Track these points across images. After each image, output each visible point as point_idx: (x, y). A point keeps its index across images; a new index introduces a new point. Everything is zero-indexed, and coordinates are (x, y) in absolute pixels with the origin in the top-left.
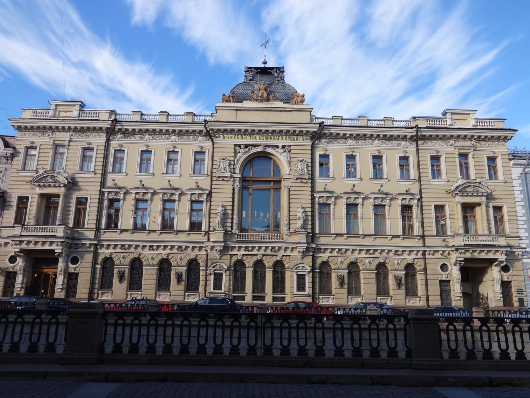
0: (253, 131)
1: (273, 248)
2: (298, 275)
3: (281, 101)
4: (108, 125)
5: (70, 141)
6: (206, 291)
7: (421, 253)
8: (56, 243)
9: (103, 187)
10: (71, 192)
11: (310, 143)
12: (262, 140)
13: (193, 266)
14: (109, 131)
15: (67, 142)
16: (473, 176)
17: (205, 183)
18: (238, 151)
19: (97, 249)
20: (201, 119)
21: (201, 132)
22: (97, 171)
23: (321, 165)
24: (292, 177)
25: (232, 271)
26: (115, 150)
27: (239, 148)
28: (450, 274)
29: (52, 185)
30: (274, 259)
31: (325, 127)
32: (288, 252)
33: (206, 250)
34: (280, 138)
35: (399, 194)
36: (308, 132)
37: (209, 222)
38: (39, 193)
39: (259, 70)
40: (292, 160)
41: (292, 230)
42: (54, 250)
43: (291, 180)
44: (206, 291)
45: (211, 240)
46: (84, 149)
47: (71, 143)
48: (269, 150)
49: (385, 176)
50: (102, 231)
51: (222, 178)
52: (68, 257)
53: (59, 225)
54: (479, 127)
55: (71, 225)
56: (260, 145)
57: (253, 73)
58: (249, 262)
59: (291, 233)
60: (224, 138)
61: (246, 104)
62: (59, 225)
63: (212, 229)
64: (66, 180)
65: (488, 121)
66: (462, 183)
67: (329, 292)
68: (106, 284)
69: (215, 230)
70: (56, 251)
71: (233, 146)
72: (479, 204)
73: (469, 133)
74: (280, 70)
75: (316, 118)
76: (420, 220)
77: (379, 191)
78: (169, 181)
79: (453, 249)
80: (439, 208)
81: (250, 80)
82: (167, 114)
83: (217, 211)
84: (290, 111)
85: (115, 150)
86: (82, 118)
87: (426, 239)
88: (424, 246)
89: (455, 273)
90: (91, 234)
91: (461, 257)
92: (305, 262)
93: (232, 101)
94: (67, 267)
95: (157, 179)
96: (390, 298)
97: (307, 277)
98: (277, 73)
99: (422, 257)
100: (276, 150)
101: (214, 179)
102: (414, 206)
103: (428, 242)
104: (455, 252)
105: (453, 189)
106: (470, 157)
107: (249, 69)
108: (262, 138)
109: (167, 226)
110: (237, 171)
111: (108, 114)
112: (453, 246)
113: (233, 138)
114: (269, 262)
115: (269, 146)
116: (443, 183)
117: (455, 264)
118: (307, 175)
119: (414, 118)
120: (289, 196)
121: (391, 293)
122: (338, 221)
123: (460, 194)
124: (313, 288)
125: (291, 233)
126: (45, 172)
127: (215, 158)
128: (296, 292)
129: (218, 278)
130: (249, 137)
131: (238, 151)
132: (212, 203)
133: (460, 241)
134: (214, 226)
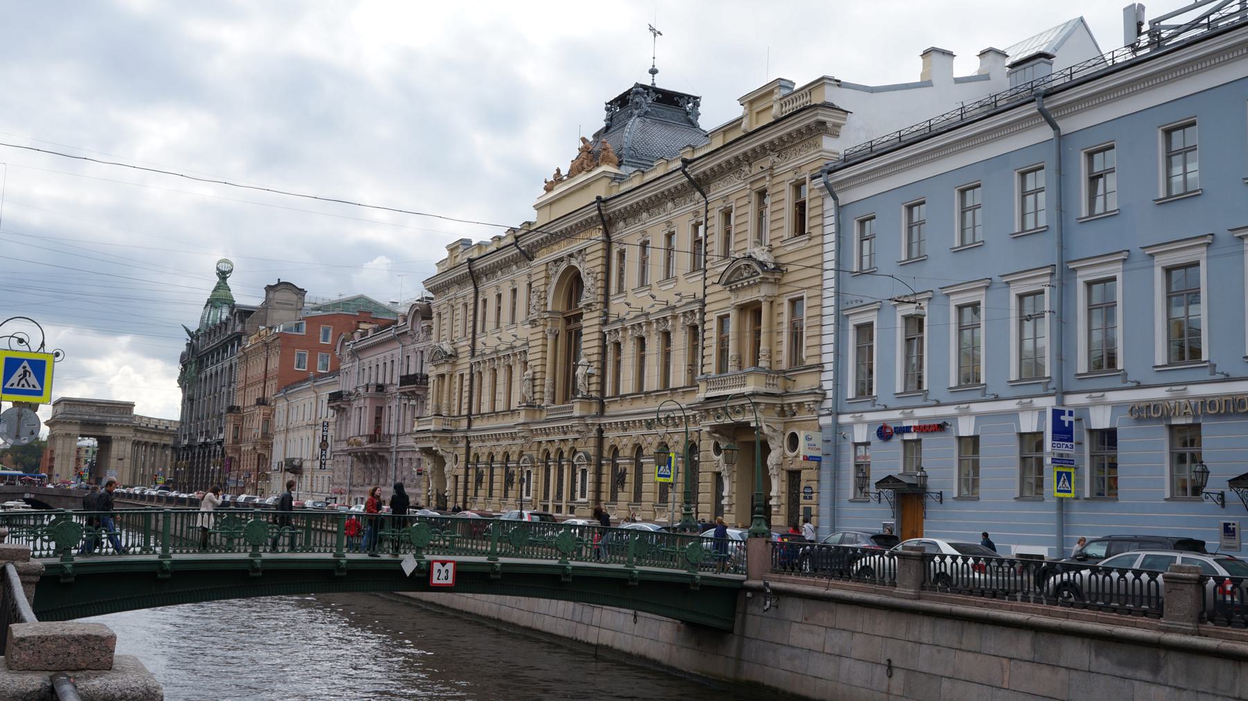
19: (468, 442)
32: (577, 436)
48: (574, 262)
71: (544, 267)
80: (723, 320)
84: (588, 186)
90: (464, 424)
124: (598, 491)
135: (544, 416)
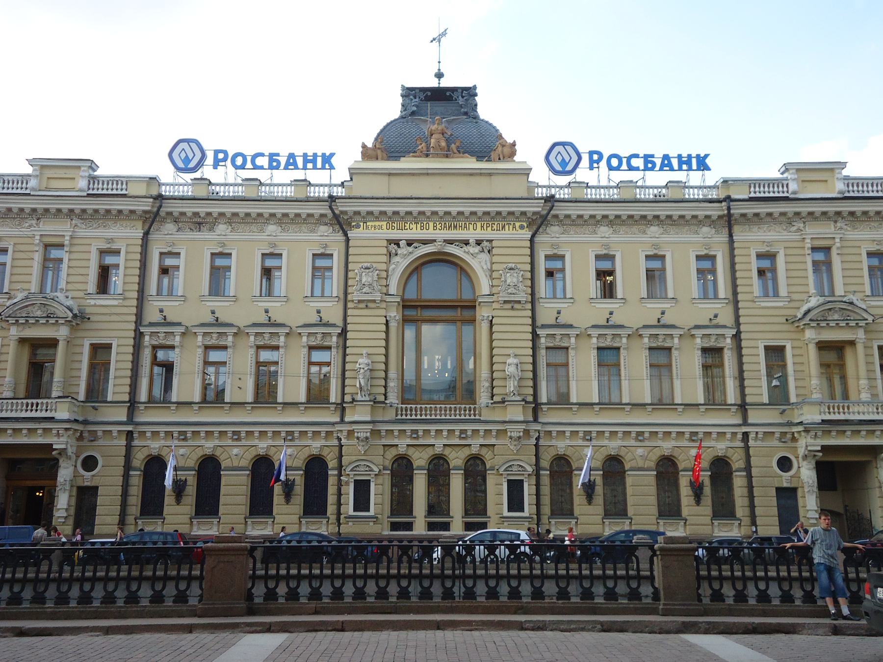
0: (422, 213)
1: (463, 432)
2: (510, 482)
3: (472, 153)
4: (147, 205)
5: (72, 237)
6: (339, 514)
7: (740, 436)
8: (54, 432)
9: (141, 325)
10: (80, 334)
11: (527, 234)
12: (438, 231)
13: (315, 468)
14: (147, 216)
15: (67, 238)
16: (839, 290)
17: (333, 314)
18: (394, 251)
20: (324, 193)
21: (322, 215)
22: (128, 294)
23: (550, 274)
24: (494, 298)
25: (387, 477)
26: (161, 254)
27: (395, 247)
28: (797, 476)
29: (43, 321)
30: (466, 452)
31: (556, 204)
32: (492, 441)
33: (340, 439)
34: (471, 226)
35: (697, 327)
36: (524, 213)
37: (343, 386)
38: (17, 338)
39: (429, 94)
40: (495, 267)
41: (496, 399)
42: (52, 445)
43: (495, 305)
44: (339, 514)
45: (347, 419)
46: (103, 252)
47: (76, 241)
49: (670, 294)
50: (142, 407)
51: (366, 304)
52: (78, 457)
53: (59, 397)
54: (851, 194)
55: (82, 397)
56: (435, 241)
57: (417, 100)
58: (420, 459)
59: (495, 403)
60: (367, 227)
61: (406, 164)
62: (59, 397)
63: (348, 398)
64: (68, 312)
65: (870, 182)
66: (818, 303)
67: (570, 514)
68: (152, 505)
69: (354, 400)
70: (54, 447)
71: (385, 243)
72: (852, 343)
73: (831, 208)
74: (469, 93)
75: (538, 186)
76: (737, 374)
77: (659, 322)
78: (267, 311)
79: (801, 428)
80: (775, 353)
81: (413, 113)
82: (258, 183)
83: (358, 366)
84: (490, 175)
85: (161, 254)
86: (95, 192)
87: (749, 412)
88: (745, 423)
89: (807, 474)
91: (816, 444)
92: (522, 458)
93: (380, 157)
94: (76, 475)
95: (243, 304)
96: (682, 522)
97: (526, 485)
98: (463, 97)
99: (742, 445)
100: (465, 248)
101: (350, 305)
102: (725, 351)
103: (754, 416)
104: (803, 434)
105: (799, 316)
106: (834, 252)
107: (409, 93)
108: (438, 226)
109: (265, 392)
110: (393, 290)
111: (145, 185)
112: (801, 423)
113: (384, 227)
114: (457, 459)
115: (450, 242)
116: (781, 304)
117: (805, 457)
118: (523, 294)
119: (725, 182)
120: (491, 333)
121: (685, 512)
122: (584, 378)
123: (814, 324)
124: (538, 504)
125: (495, 403)
126: (27, 298)
127: (350, 267)
128: (506, 513)
129: (362, 489)
130: (413, 226)
131: (394, 251)
132: (348, 351)
133: (811, 415)
134: (352, 394)
135: (390, 415)
